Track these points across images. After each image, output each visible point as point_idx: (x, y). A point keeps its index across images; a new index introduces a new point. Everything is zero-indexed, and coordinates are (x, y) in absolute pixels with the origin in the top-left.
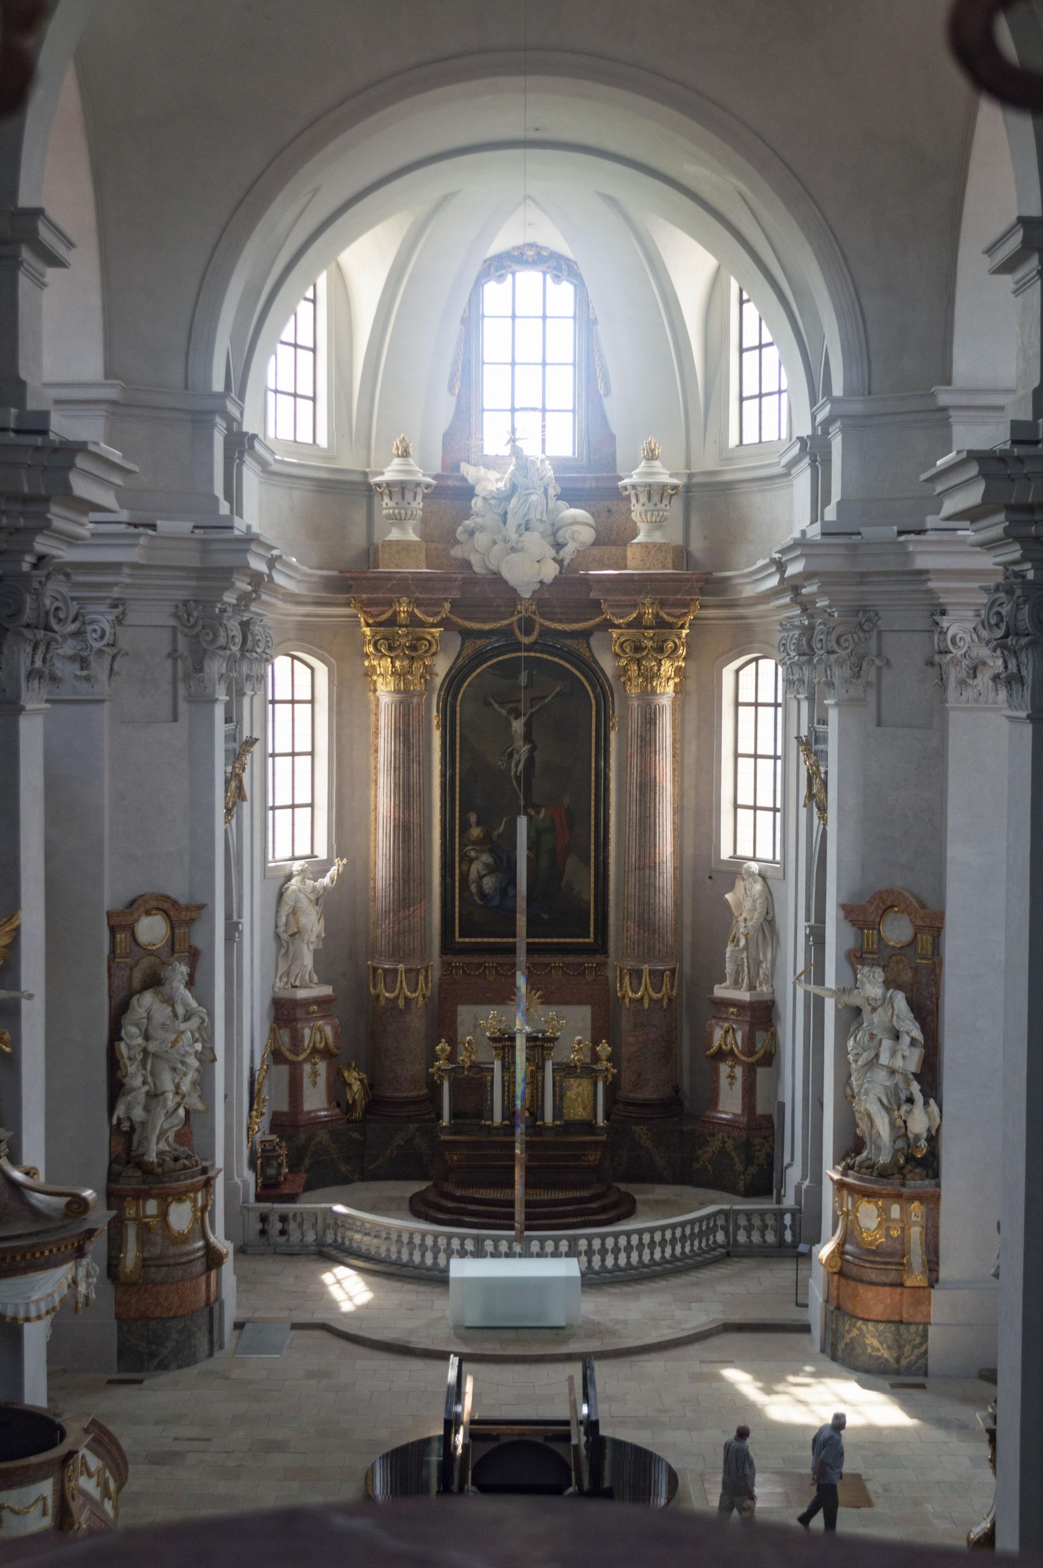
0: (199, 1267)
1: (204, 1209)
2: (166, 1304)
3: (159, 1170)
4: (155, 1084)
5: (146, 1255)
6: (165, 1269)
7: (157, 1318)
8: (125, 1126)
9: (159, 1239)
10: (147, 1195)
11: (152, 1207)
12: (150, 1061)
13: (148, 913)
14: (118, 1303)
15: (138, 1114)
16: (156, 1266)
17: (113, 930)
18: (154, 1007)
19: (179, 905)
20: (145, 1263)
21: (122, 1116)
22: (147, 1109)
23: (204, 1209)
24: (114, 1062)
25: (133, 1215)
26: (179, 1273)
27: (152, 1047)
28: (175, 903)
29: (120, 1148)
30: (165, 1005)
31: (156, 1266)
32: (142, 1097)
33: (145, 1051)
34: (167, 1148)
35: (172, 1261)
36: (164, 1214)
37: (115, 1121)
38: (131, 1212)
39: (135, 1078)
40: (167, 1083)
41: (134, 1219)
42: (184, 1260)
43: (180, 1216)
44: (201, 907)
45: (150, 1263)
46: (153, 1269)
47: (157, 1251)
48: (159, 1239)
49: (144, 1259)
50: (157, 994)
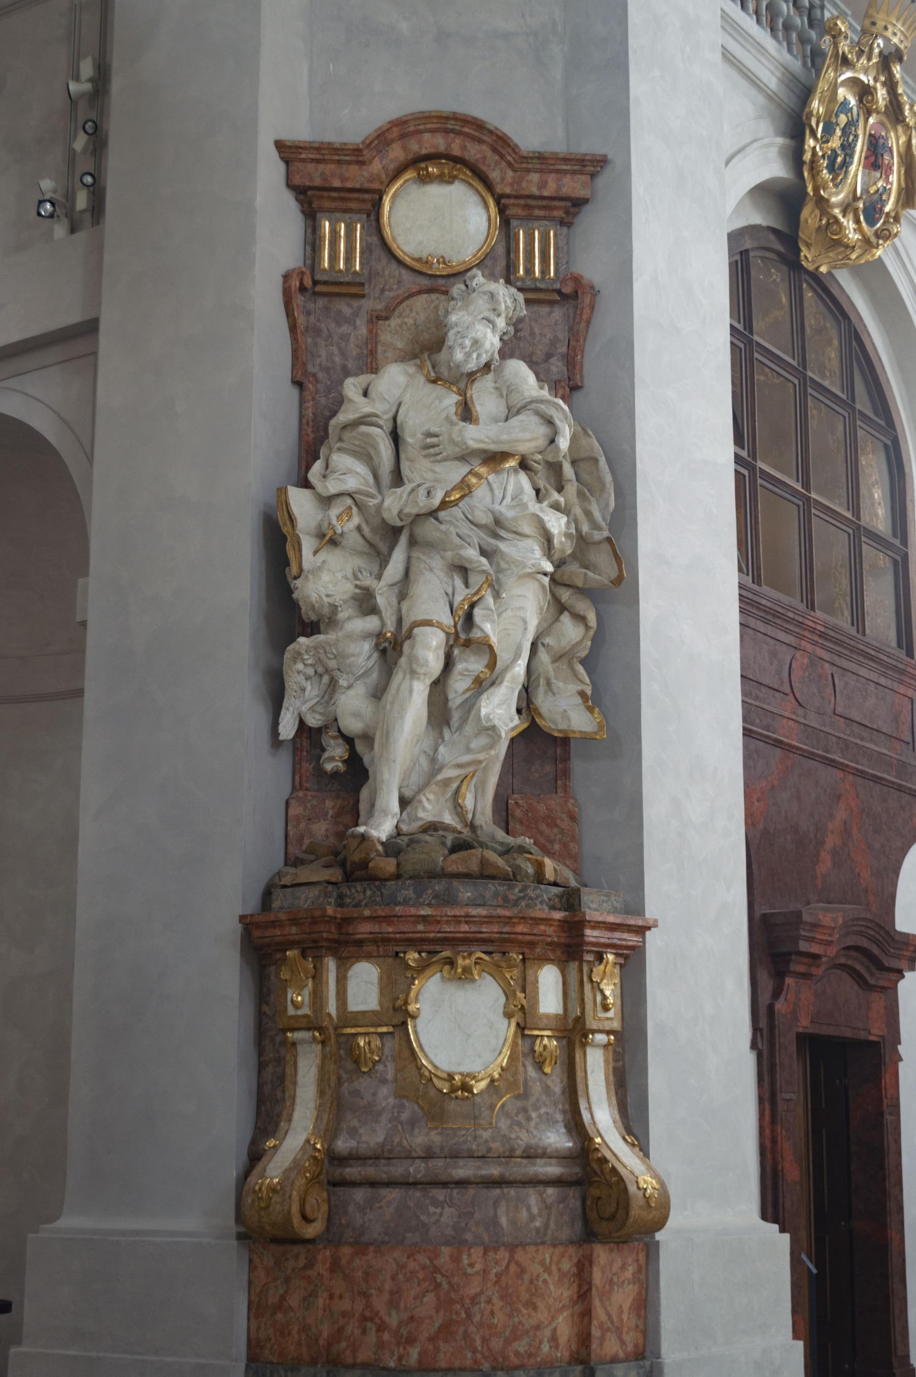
0: (532, 1210)
1: (573, 1032)
2: (393, 1320)
3: (389, 865)
4: (400, 621)
5: (343, 1145)
6: (392, 1195)
7: (365, 1366)
8: (334, 756)
9: (385, 1097)
10: (347, 948)
11: (364, 985)
12: (398, 557)
13: (417, 163)
14: (256, 1309)
15: (353, 707)
16: (373, 1184)
17: (311, 200)
18: (407, 399)
19: (515, 149)
20: (332, 1171)
21: (313, 721)
22: (378, 694)
23: (573, 1032)
24: (277, 542)
25: (306, 1010)
26: (442, 1214)
27: (393, 504)
28: (501, 143)
29: (321, 829)
30: (439, 389)
31: (373, 1184)
32: (362, 654)
33: (393, 533)
34: (448, 819)
35: (417, 1169)
36: (397, 1015)
37: (287, 729)
38: (299, 999)
39: (326, 579)
40: (433, 599)
41: (310, 1025)
42: (464, 1170)
43: (461, 1027)
44: (592, 166)
45: (351, 1172)
46: (359, 1195)
47: (373, 1136)
48: (385, 1097)
49: (335, 1159)
50: (420, 367)
